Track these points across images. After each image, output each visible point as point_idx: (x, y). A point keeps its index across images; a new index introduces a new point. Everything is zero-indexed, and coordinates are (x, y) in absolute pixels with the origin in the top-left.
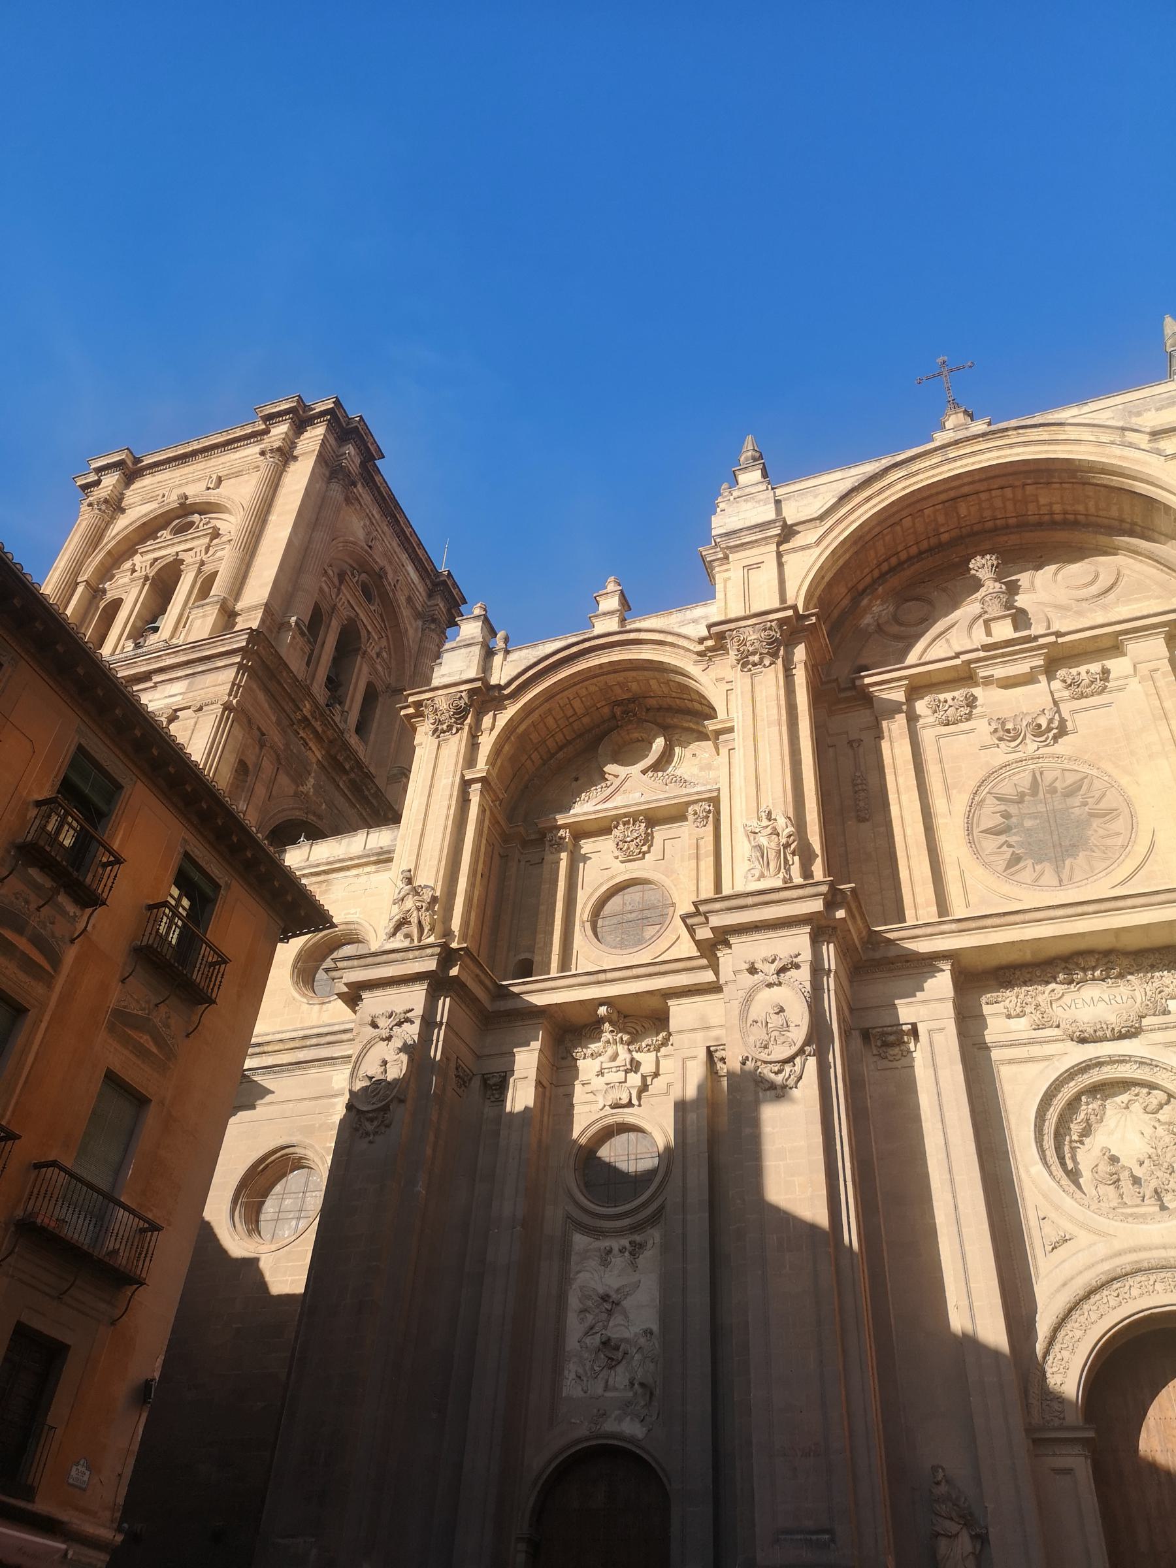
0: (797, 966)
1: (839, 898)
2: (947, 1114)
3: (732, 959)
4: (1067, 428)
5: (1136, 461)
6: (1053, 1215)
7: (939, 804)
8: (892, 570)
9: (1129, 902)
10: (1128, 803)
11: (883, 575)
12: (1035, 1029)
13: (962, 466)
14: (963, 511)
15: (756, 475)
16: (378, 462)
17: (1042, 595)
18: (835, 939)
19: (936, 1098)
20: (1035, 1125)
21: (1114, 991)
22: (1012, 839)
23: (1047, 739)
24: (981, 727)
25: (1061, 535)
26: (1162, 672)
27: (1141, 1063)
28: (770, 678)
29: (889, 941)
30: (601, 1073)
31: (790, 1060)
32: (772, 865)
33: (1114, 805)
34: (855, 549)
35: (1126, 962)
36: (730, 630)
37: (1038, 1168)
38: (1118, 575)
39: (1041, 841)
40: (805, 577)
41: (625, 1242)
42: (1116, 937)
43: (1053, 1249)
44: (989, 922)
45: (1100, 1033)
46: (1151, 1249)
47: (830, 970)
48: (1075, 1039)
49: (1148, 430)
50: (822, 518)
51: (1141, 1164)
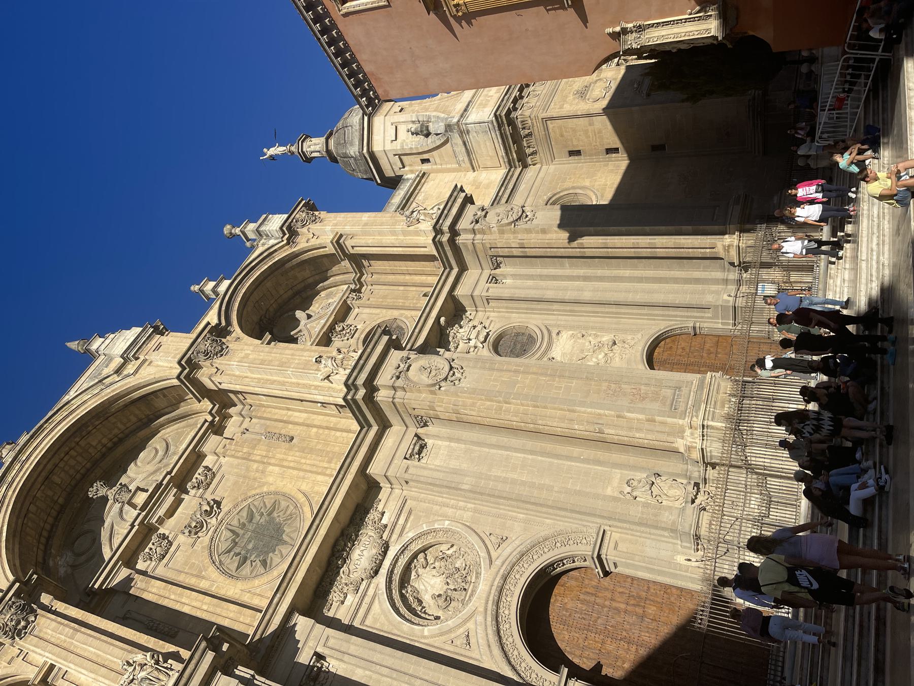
1: (216, 642)
2: (374, 660)
4: (72, 402)
5: (120, 387)
6: (453, 635)
7: (203, 585)
8: (48, 539)
9: (326, 503)
10: (276, 493)
12: (357, 593)
13: (36, 457)
14: (58, 481)
17: (141, 477)
21: (361, 543)
22: (252, 558)
23: (215, 511)
25: (120, 449)
26: (229, 444)
27: (402, 552)
29: (260, 640)
32: (161, 677)
33: (273, 501)
34: (17, 540)
37: (426, 631)
38: (164, 440)
39: (264, 545)
42: (338, 522)
43: (469, 643)
44: (289, 575)
46: (490, 593)
47: (253, 676)
48: (373, 575)
49: (112, 372)
51: (448, 584)
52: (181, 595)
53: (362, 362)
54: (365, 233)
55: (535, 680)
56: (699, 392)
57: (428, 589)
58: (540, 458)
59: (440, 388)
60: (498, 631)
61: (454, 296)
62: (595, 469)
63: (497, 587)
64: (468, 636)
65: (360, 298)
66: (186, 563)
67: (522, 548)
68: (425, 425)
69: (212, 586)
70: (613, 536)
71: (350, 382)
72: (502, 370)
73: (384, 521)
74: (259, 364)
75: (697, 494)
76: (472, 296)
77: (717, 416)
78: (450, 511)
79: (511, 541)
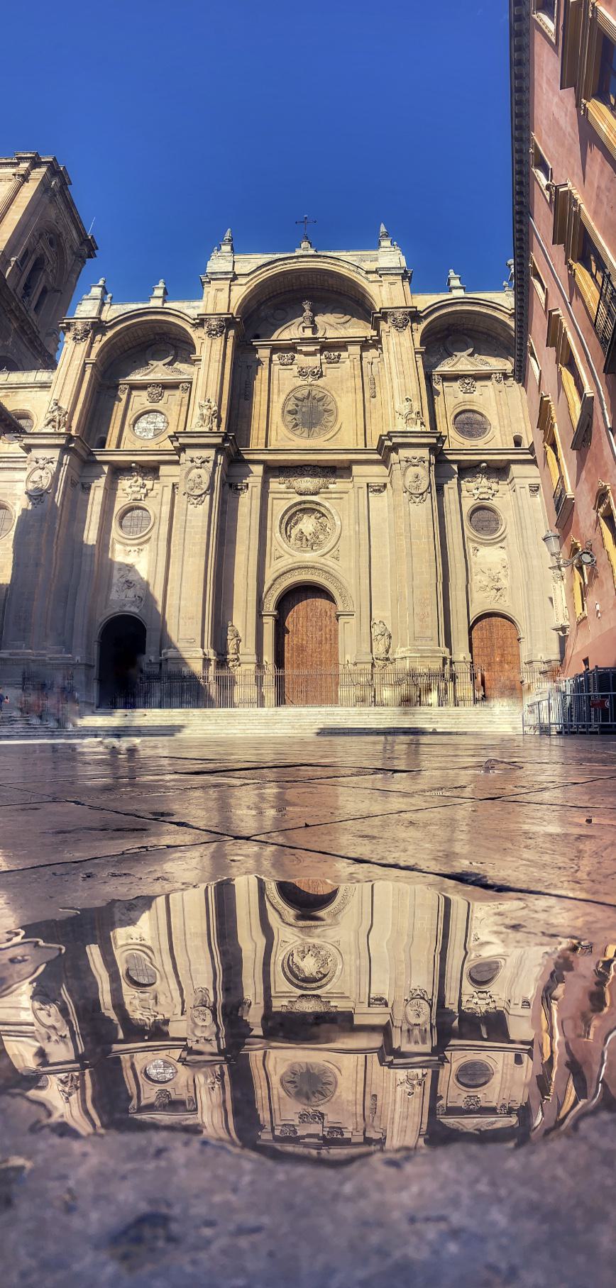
0: (208, 462)
6: (279, 549)
7: (274, 397)
11: (270, 298)
15: (228, 248)
22: (297, 417)
28: (219, 341)
30: (131, 487)
31: (200, 496)
32: (207, 421)
41: (136, 548)
50: (249, 274)
52: (264, 391)
60: (285, 573)
70: (353, 620)
71: (391, 434)
73: (331, 486)
78: (346, 522)
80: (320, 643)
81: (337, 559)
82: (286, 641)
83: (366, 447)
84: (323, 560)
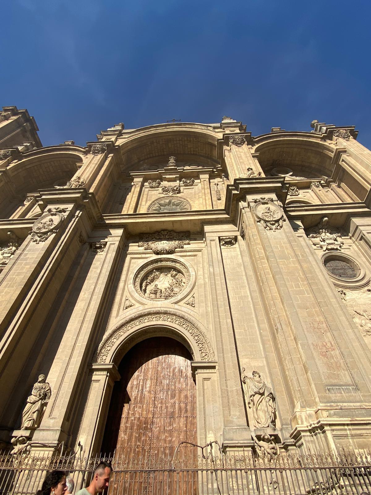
0: (65, 212)
3: (46, 210)
5: (209, 133)
6: (130, 299)
7: (143, 203)
9: (178, 214)
12: (145, 250)
16: (37, 131)
18: (84, 209)
19: (103, 260)
20: (135, 274)
24: (160, 189)
28: (100, 157)
31: (46, 233)
35: (175, 234)
36: (93, 145)
37: (131, 286)
40: (122, 143)
42: (173, 224)
45: (162, 251)
46: (156, 308)
51: (166, 289)
52: (135, 197)
53: (254, 181)
54: (356, 158)
55: (107, 349)
56: (364, 411)
57: (160, 283)
58: (252, 305)
59: (258, 222)
60: (132, 320)
61: (350, 218)
62: (259, 345)
63: (159, 311)
64: (131, 306)
65: (318, 187)
66: (151, 195)
67: (186, 316)
68: (243, 236)
69: (143, 205)
70: (214, 375)
72: (292, 248)
73: (185, 246)
74: (238, 157)
75: (268, 441)
76: (357, 227)
77: (344, 441)
78: (200, 273)
79: (193, 310)
80: (172, 416)
81: (192, 305)
82: (124, 415)
83: (213, 208)
84: (176, 306)
